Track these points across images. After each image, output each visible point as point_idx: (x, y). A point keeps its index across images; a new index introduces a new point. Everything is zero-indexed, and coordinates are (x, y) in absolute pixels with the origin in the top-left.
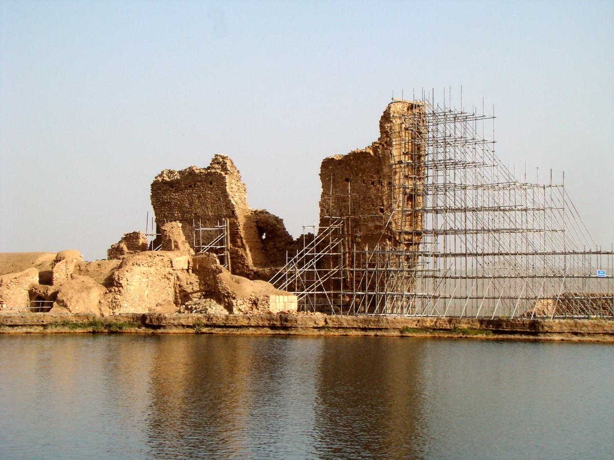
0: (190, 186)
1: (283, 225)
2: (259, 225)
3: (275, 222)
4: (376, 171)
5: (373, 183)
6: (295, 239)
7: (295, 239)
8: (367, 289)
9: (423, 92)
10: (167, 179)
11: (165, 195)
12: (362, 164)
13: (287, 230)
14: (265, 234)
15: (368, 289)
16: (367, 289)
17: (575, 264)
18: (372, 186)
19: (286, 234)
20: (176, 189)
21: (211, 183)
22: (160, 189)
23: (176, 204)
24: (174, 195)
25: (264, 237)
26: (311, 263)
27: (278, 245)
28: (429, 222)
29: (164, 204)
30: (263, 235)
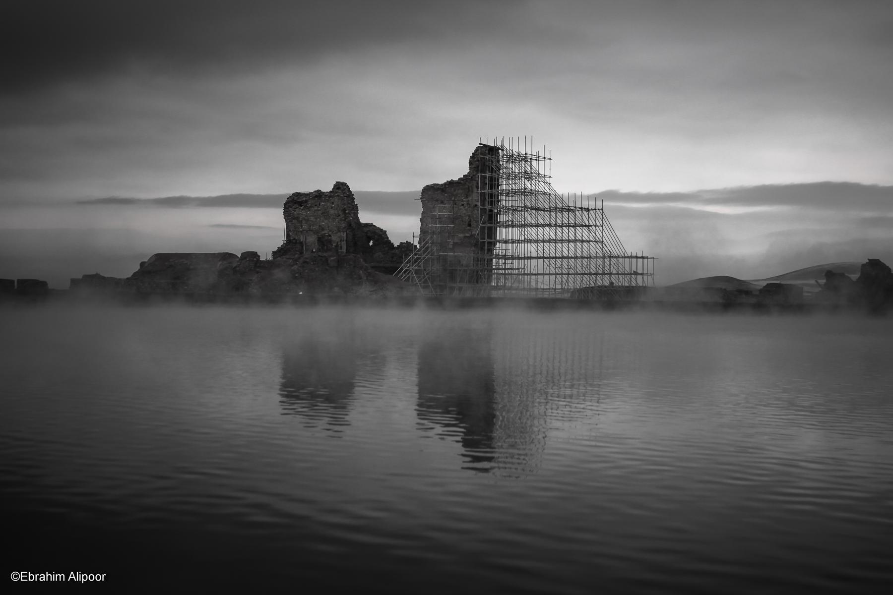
0: (316, 205)
1: (386, 235)
2: (368, 235)
3: (381, 233)
4: (465, 196)
5: (463, 205)
6: (396, 246)
7: (396, 246)
8: (458, 281)
9: (503, 141)
11: (295, 211)
12: (455, 191)
13: (389, 239)
14: (372, 242)
15: (459, 282)
16: (458, 281)
17: (626, 266)
18: (462, 207)
19: (389, 242)
20: (304, 208)
22: (291, 207)
23: (304, 219)
25: (371, 243)
26: (419, 263)
28: (502, 233)
30: (370, 242)
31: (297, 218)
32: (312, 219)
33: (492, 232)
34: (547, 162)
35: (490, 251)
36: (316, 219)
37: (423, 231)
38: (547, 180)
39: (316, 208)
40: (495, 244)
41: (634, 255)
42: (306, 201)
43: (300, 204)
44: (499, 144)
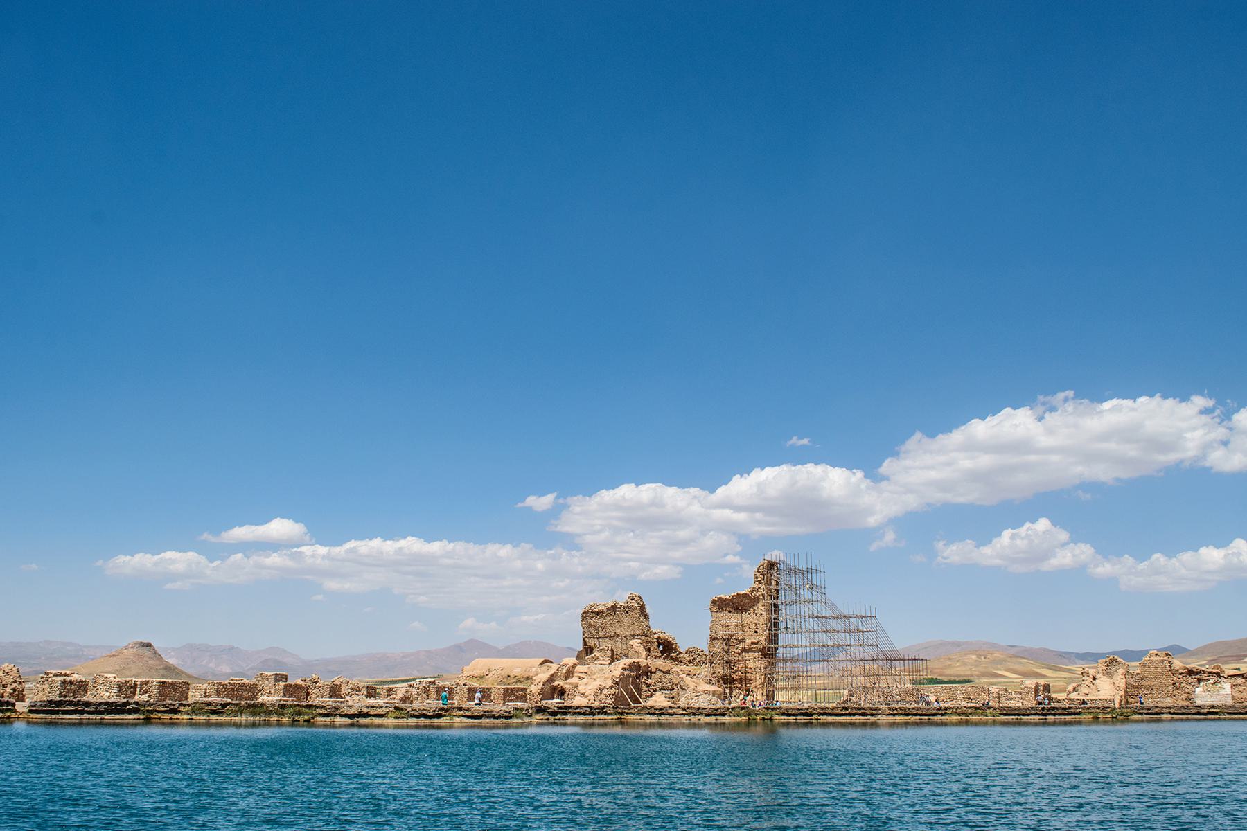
5: (749, 614)
10: (592, 608)
21: (627, 613)
24: (600, 621)
25: (661, 648)
27: (672, 654)
29: (590, 626)
31: (595, 626)
32: (608, 626)
33: (773, 639)
34: (822, 574)
35: (773, 656)
36: (612, 627)
37: (713, 639)
38: (823, 590)
39: (612, 617)
40: (776, 649)
41: (914, 658)
42: (603, 612)
43: (597, 613)
44: (778, 562)
